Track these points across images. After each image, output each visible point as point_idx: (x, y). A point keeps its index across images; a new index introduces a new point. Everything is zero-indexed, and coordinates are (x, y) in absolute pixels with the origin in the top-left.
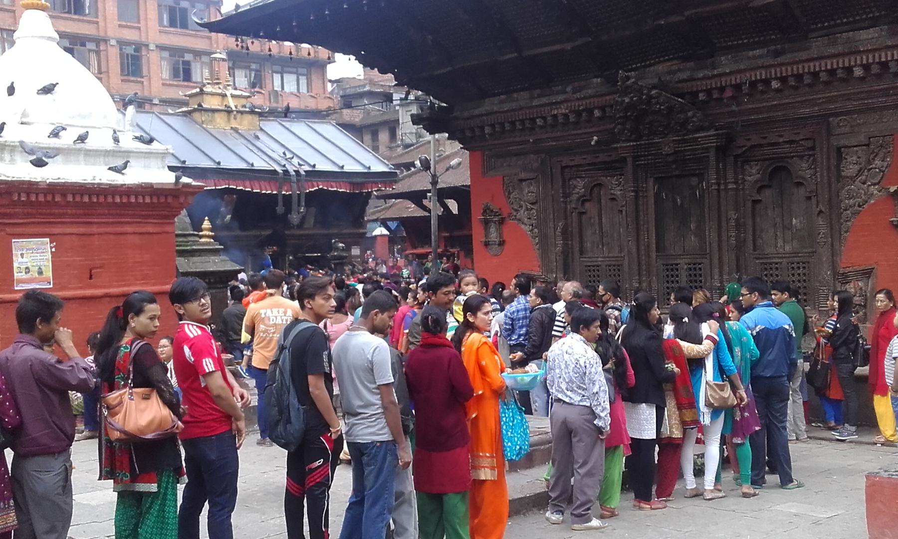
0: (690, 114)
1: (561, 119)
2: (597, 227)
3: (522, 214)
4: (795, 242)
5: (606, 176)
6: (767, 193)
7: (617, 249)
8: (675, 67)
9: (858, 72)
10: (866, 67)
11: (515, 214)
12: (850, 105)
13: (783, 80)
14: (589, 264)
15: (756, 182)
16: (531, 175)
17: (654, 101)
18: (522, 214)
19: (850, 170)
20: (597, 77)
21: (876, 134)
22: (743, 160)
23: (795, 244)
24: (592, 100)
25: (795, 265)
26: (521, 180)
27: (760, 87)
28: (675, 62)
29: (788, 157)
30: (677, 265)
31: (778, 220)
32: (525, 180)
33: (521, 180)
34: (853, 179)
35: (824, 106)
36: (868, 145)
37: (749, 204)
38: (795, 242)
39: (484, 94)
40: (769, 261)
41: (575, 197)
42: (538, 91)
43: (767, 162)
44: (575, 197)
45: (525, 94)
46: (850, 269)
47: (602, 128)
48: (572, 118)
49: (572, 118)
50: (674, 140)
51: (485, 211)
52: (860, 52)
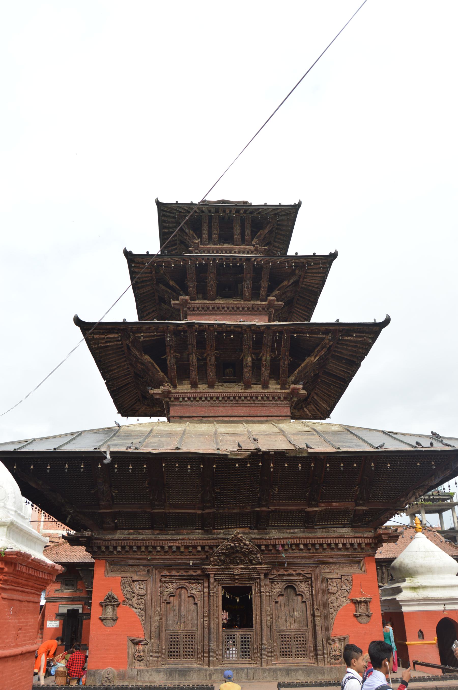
0: (258, 556)
1: (174, 549)
2: (177, 612)
3: (134, 601)
4: (296, 624)
5: (189, 583)
6: (281, 598)
7: (190, 625)
8: (247, 531)
9: (340, 546)
10: (344, 545)
11: (127, 601)
12: (331, 560)
13: (306, 545)
14: (171, 634)
15: (278, 593)
16: (142, 578)
17: (245, 547)
18: (134, 601)
20: (199, 529)
21: (344, 574)
22: (273, 581)
23: (296, 625)
24: (198, 541)
25: (298, 636)
26: (134, 581)
27: (294, 547)
28: (248, 529)
29: (295, 581)
30: (234, 635)
31: (287, 612)
32: (136, 581)
33: (134, 581)
35: (320, 559)
37: (274, 603)
38: (296, 624)
39: (116, 528)
40: (284, 633)
42: (158, 532)
43: (285, 583)
44: (166, 594)
45: (149, 532)
46: (336, 637)
47: (197, 557)
48: (182, 549)
49: (182, 549)
50: (241, 568)
51: (108, 598)
52: (345, 538)
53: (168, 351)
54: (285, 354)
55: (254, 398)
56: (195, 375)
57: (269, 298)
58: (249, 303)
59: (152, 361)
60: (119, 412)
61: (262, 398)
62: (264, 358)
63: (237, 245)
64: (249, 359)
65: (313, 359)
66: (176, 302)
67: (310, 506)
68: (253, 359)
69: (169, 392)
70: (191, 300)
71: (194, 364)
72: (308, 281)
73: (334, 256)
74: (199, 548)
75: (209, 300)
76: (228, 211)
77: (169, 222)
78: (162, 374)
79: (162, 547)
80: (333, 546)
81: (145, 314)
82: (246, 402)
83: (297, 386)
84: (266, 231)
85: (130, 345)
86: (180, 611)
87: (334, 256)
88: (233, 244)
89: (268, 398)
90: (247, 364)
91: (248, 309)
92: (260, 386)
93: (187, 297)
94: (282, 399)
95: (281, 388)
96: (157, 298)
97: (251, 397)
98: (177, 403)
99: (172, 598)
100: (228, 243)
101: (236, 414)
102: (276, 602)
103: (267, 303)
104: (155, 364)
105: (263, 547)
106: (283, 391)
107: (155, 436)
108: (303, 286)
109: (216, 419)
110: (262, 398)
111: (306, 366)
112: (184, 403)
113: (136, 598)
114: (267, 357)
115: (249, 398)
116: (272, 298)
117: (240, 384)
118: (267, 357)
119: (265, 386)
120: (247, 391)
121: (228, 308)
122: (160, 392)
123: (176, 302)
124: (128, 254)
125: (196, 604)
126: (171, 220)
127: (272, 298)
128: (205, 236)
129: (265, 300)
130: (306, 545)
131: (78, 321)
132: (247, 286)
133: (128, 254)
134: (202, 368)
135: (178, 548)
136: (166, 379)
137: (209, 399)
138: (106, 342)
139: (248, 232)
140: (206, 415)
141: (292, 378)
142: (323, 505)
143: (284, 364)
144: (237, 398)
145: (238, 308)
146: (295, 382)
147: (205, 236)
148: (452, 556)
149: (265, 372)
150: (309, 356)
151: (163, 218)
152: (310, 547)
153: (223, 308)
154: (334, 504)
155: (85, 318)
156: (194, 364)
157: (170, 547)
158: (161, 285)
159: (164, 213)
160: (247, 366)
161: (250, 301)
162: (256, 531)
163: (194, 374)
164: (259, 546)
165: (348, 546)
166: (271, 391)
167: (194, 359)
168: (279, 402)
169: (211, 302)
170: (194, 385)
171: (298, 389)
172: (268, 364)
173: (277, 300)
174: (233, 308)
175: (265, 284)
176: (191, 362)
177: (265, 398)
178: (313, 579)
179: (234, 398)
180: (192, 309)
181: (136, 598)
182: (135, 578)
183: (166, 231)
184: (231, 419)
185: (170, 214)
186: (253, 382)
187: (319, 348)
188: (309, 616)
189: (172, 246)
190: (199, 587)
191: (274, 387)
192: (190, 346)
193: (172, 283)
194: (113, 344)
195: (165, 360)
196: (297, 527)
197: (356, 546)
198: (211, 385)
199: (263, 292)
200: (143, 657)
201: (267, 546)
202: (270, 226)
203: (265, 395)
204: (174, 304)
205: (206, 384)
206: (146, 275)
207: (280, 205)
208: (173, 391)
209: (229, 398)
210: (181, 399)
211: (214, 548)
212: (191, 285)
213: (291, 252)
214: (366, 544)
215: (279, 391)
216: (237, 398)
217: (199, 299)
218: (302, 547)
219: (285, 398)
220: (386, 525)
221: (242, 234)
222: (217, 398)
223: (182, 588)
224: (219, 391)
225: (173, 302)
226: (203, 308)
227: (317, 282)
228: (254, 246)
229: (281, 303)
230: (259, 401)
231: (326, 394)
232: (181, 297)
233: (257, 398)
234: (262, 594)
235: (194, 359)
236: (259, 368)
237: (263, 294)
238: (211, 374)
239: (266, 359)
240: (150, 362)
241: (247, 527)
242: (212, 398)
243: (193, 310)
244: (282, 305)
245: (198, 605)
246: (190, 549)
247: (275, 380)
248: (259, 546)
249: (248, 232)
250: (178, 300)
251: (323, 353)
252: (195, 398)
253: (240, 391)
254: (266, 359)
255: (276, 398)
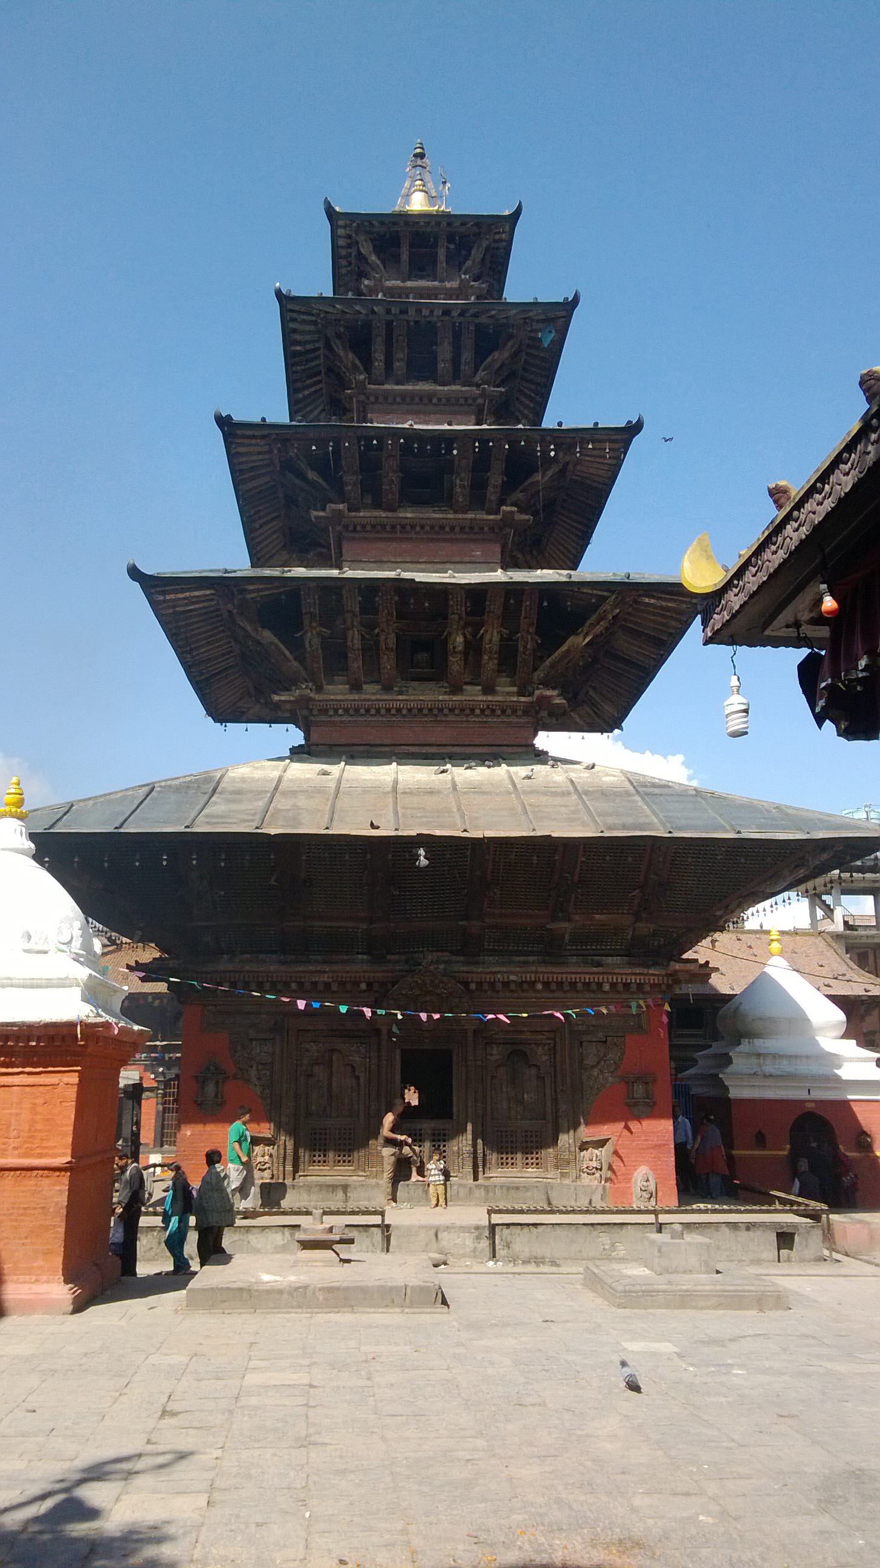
8: (446, 958)
9: (607, 987)
10: (613, 985)
13: (546, 984)
17: (441, 985)
18: (253, 1072)
19: (590, 1061)
27: (525, 986)
34: (593, 1067)
36: (605, 1042)
37: (489, 1079)
41: (305, 1062)
44: (305, 1062)
49: (334, 987)
51: (208, 1069)
53: (306, 622)
54: (528, 632)
55: (467, 712)
56: (358, 667)
57: (504, 508)
58: (465, 516)
59: (276, 640)
60: (210, 713)
61: (482, 711)
62: (487, 637)
63: (443, 385)
64: (460, 639)
65: (580, 640)
66: (322, 514)
67: (554, 919)
68: (466, 641)
69: (311, 699)
70: (350, 510)
71: (356, 647)
72: (583, 469)
73: (634, 429)
74: (363, 986)
75: (385, 510)
76: (425, 312)
77: (303, 332)
78: (295, 664)
79: (301, 984)
80: (594, 987)
81: (257, 525)
82: (452, 718)
83: (549, 693)
84: (506, 354)
85: (235, 611)
86: (330, 1085)
87: (634, 429)
88: (436, 382)
89: (493, 711)
90: (454, 648)
91: (462, 528)
92: (479, 688)
93: (341, 506)
94: (520, 713)
95: (520, 694)
96: (281, 495)
97: (462, 710)
98: (323, 718)
99: (316, 1069)
100: (425, 379)
101: (433, 740)
102: (493, 1077)
103: (499, 517)
104: (281, 646)
105: (473, 986)
106: (523, 699)
107: (285, 794)
108: (574, 477)
109: (397, 749)
110: (482, 711)
111: (568, 651)
112: (338, 719)
113: (254, 1067)
114: (492, 636)
115: (457, 712)
116: (509, 508)
117: (442, 684)
118: (492, 636)
119: (489, 689)
120: (455, 698)
121: (422, 527)
122: (292, 698)
123: (322, 514)
124: (223, 422)
125: (358, 1078)
126: (308, 328)
127: (509, 508)
128: (379, 364)
129: (497, 512)
130: (546, 984)
131: (134, 573)
132: (461, 483)
133: (223, 422)
134: (371, 651)
135: (327, 985)
136: (303, 673)
137: (383, 712)
138: (187, 605)
139: (467, 356)
140: (378, 742)
141: (540, 674)
142: (577, 917)
143: (525, 647)
144: (436, 712)
145: (442, 528)
146: (546, 683)
147: (379, 364)
148: (834, 999)
149: (490, 664)
150: (574, 632)
151: (292, 325)
152: (553, 987)
153: (413, 527)
154: (597, 916)
155: (148, 570)
156: (356, 647)
157: (315, 984)
158: (290, 476)
159: (294, 315)
160: (455, 652)
161: (465, 512)
162: (462, 958)
163: (356, 664)
164: (466, 984)
165: (620, 988)
166: (500, 698)
167: (355, 639)
168: (513, 719)
169: (390, 514)
170: (356, 687)
171: (550, 697)
172: (495, 648)
173: (520, 511)
174: (432, 527)
175: (496, 479)
176: (349, 644)
177: (487, 712)
178: (558, 1040)
179: (430, 710)
180: (351, 528)
181: (254, 1067)
182: (252, 1034)
183: (299, 348)
184: (425, 750)
185: (305, 317)
186: (467, 680)
187: (593, 619)
188: (549, 1103)
189: (309, 377)
190: (363, 1051)
191: (506, 692)
192: (348, 616)
193: (312, 475)
194: (201, 605)
195: (302, 638)
196: (532, 953)
197: (634, 988)
198: (387, 688)
199: (492, 495)
200: (267, 1165)
201: (480, 984)
202: (513, 346)
203: (488, 707)
204: (316, 518)
205: (377, 682)
206: (260, 457)
207: (536, 304)
208: (317, 697)
209: (420, 710)
210: (331, 713)
211: (389, 986)
212: (351, 481)
213: (549, 422)
214: (653, 986)
215: (515, 699)
216: (436, 712)
217: (366, 507)
218: (539, 986)
219: (526, 713)
220: (685, 956)
221: (456, 361)
222: (399, 710)
223: (332, 1050)
224: (400, 697)
225: (314, 513)
226: (373, 526)
227: (601, 473)
228: (478, 386)
229: (527, 517)
230: (477, 716)
231: (613, 690)
232: (331, 506)
233: (472, 710)
234: (470, 1063)
235: (355, 639)
236: (479, 652)
237: (493, 498)
238: (388, 662)
239: (491, 640)
240: (272, 643)
241: (446, 951)
242: (388, 710)
243: (355, 530)
244: (528, 520)
245: (362, 1080)
246: (349, 987)
247: (508, 676)
248: (466, 984)
249: (467, 356)
250: (324, 509)
251: (599, 629)
252: (357, 710)
253: (441, 698)
254: (491, 640)
255: (509, 712)
